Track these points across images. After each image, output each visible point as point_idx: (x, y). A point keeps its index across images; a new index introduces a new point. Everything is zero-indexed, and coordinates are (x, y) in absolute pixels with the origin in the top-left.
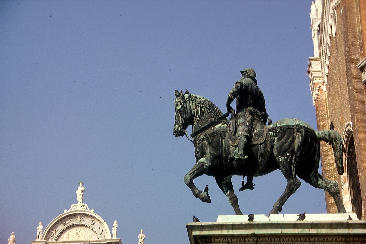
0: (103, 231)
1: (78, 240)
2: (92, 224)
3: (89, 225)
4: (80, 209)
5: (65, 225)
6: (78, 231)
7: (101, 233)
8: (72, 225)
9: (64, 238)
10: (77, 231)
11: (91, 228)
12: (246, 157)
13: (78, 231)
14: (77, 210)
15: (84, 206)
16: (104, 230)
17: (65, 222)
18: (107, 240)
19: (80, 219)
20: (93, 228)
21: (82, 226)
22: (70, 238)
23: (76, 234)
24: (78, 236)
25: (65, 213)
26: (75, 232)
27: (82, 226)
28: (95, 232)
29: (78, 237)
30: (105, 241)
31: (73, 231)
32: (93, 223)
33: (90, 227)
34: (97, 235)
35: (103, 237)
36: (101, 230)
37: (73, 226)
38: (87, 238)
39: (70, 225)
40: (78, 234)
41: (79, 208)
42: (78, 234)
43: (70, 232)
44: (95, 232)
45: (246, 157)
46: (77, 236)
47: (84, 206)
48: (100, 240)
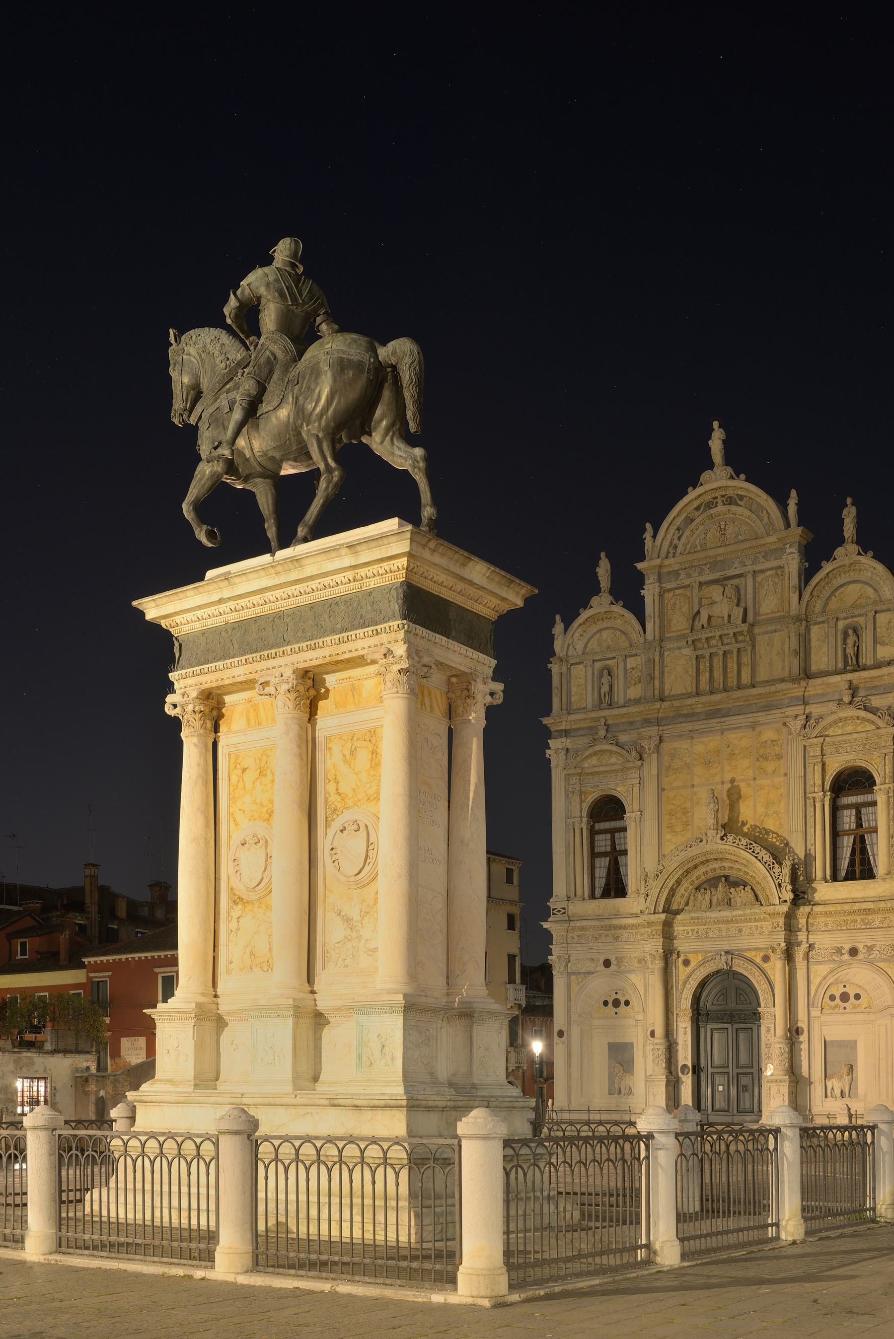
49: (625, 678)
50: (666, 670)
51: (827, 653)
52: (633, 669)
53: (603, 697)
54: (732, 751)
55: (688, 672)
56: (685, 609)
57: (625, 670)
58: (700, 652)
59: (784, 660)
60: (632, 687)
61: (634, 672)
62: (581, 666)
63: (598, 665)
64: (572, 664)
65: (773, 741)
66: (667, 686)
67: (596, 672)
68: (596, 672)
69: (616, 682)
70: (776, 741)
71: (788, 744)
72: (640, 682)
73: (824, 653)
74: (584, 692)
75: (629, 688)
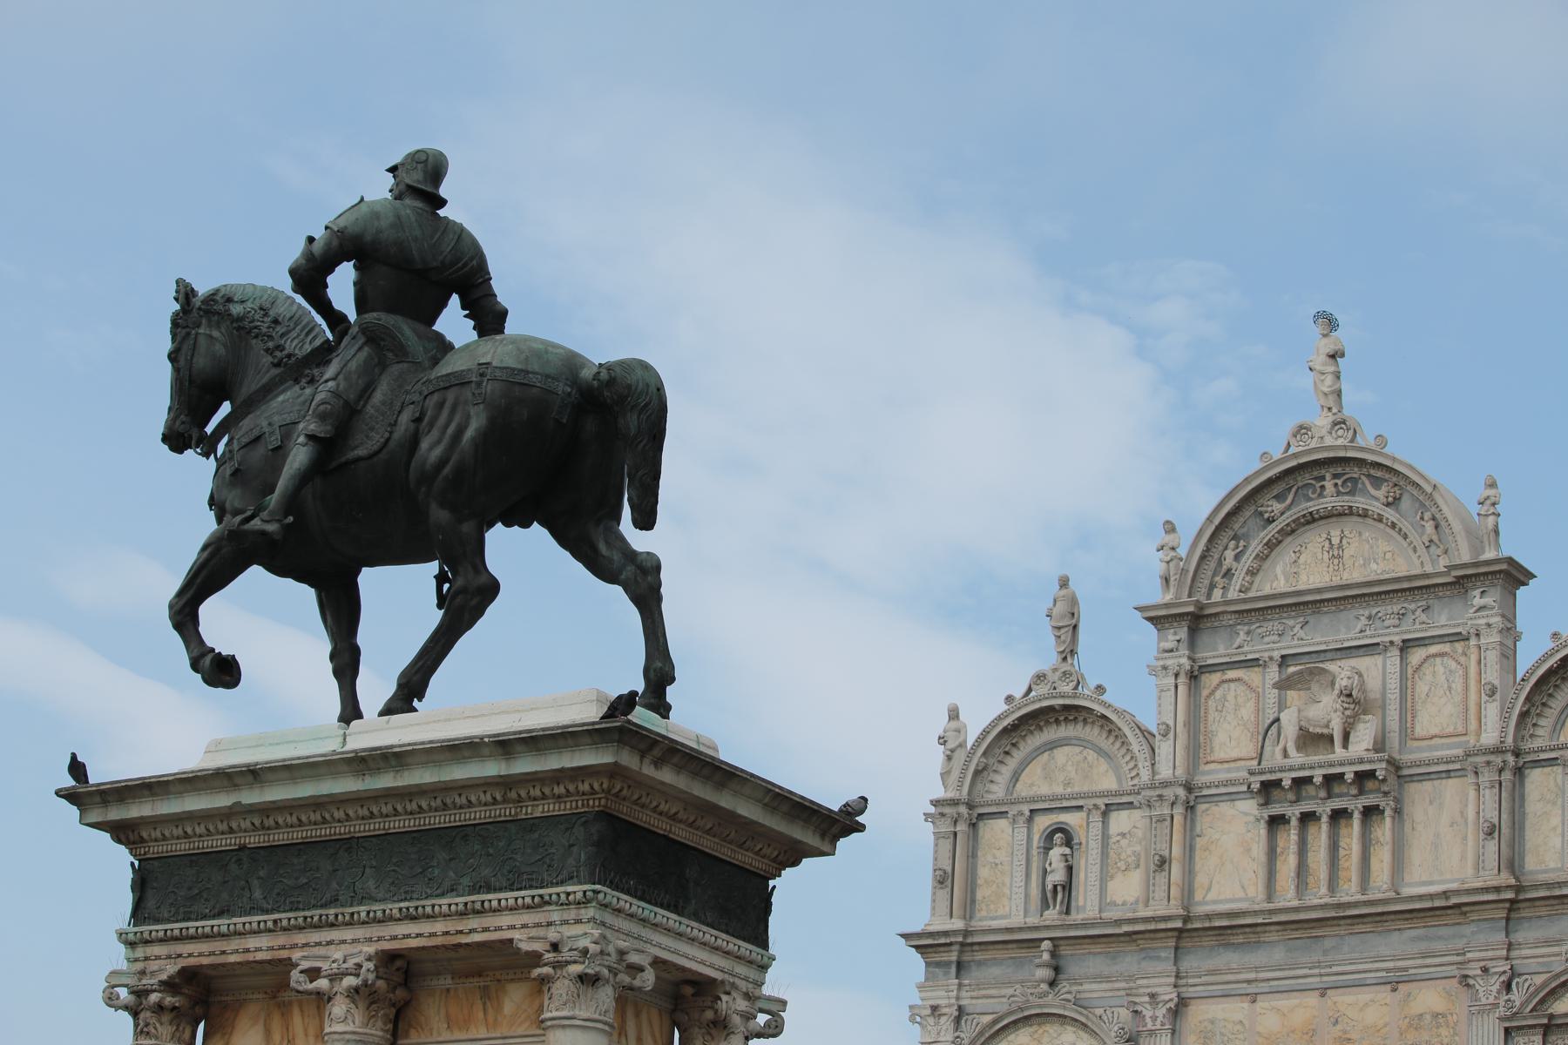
0: (1436, 527)
1: (1336, 581)
2: (1388, 505)
3: (1376, 507)
4: (1329, 441)
5: (1270, 521)
6: (1335, 541)
7: (1431, 541)
8: (1304, 516)
9: (1276, 575)
10: (1327, 542)
11: (1384, 521)
12: (291, 519)
13: (1335, 541)
14: (1313, 445)
15: (1345, 424)
16: (1443, 523)
17: (1270, 509)
18: (1455, 567)
19: (1336, 485)
20: (1395, 521)
21: (1350, 512)
22: (1303, 577)
23: (1326, 556)
24: (1336, 561)
25: (1275, 462)
26: (1323, 547)
27: (1350, 512)
28: (1405, 537)
29: (1336, 568)
30: (1447, 574)
31: (1314, 542)
32: (1390, 499)
33: (1380, 519)
34: (1415, 550)
35: (1439, 556)
36: (1429, 526)
37: (1311, 519)
38: (1374, 566)
39: (1294, 517)
40: (1336, 553)
41: (1322, 438)
42: (1336, 554)
43: (1302, 546)
44: (1405, 537)
45: (291, 519)
46: (1331, 566)
47: (1343, 426)
48: (1429, 569)
49: (1104, 854)
50: (1199, 842)
51: (1559, 830)
52: (1123, 835)
53: (1049, 895)
54: (1345, 1032)
55: (1249, 850)
56: (1247, 712)
57: (1105, 836)
58: (1276, 810)
59: (1465, 838)
60: (1119, 877)
61: (1124, 842)
62: (1002, 823)
63: (1043, 822)
64: (981, 816)
65: (1436, 1015)
66: (1201, 879)
67: (1036, 838)
68: (1036, 838)
69: (1083, 862)
70: (1444, 1016)
71: (1470, 1024)
72: (1138, 866)
73: (1554, 829)
74: (1007, 881)
75: (1112, 877)
